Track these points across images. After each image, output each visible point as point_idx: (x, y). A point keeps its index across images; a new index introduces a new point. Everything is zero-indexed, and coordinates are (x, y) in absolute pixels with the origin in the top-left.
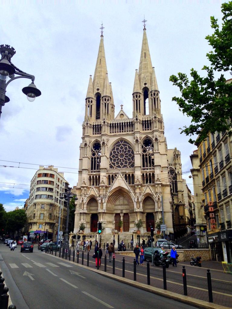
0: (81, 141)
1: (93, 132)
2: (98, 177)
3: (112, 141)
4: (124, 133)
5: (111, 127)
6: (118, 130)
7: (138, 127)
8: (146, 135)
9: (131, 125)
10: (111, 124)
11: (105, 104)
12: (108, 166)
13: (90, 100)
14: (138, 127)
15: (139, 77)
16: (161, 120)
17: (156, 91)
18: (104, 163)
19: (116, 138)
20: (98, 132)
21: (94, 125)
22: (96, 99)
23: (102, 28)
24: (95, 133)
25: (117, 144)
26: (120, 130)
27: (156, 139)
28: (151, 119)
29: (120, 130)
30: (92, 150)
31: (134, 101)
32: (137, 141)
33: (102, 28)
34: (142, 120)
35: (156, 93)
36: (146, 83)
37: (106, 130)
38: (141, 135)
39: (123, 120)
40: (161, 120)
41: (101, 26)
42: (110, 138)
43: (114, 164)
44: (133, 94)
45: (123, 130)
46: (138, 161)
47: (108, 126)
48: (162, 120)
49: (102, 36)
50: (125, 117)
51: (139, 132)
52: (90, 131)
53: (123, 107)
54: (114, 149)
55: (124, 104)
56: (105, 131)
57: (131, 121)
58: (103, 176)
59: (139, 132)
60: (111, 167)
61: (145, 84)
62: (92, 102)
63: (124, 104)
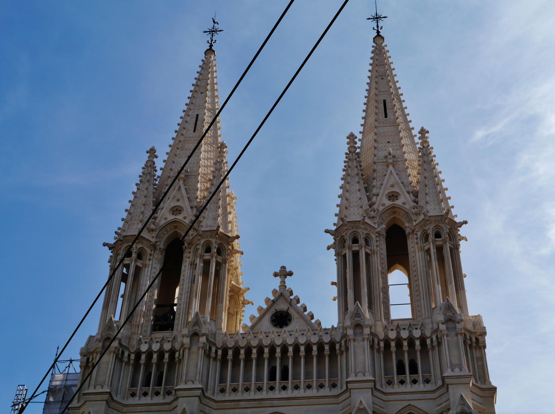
1: (133, 384)
5: (224, 362)
8: (406, 403)
9: (328, 352)
10: (225, 351)
11: (207, 263)
14: (360, 360)
15: (361, 170)
16: (477, 339)
20: (160, 384)
21: (138, 354)
23: (213, 32)
24: (139, 389)
28: (428, 333)
31: (345, 256)
33: (213, 32)
34: (382, 336)
35: (445, 230)
36: (398, 191)
38: (377, 401)
40: (477, 339)
41: (210, 26)
45: (284, 376)
47: (213, 355)
48: (480, 338)
50: (295, 325)
53: (288, 279)
57: (326, 339)
61: (393, 196)
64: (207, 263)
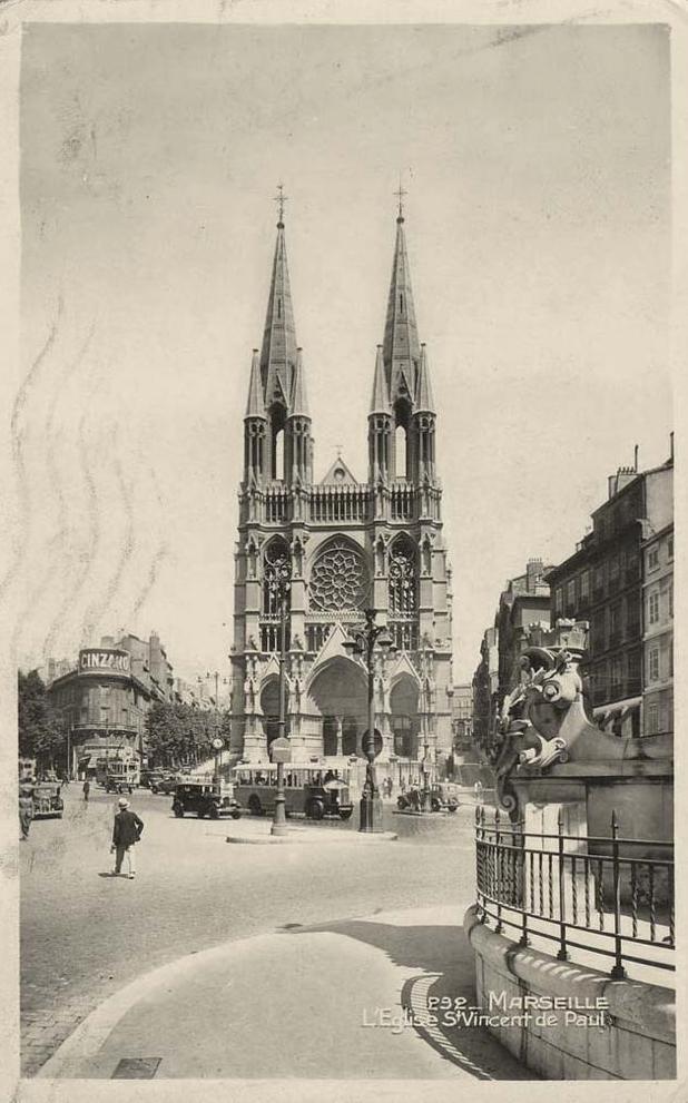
0: (237, 537)
2: (268, 630)
3: (318, 539)
4: (347, 523)
6: (331, 512)
7: (383, 511)
9: (365, 500)
12: (306, 606)
13: (258, 424)
17: (427, 414)
18: (301, 597)
19: (325, 535)
22: (270, 420)
25: (326, 549)
26: (336, 512)
27: (427, 544)
29: (336, 512)
30: (266, 563)
32: (381, 545)
37: (302, 513)
39: (343, 486)
42: (313, 536)
43: (321, 599)
44: (369, 418)
46: (381, 598)
49: (281, 226)
51: (384, 524)
52: (259, 514)
54: (321, 560)
55: (339, 443)
56: (300, 517)
58: (298, 627)
59: (384, 524)
60: (314, 606)
62: (262, 428)
63: (339, 443)
64: (299, 438)
